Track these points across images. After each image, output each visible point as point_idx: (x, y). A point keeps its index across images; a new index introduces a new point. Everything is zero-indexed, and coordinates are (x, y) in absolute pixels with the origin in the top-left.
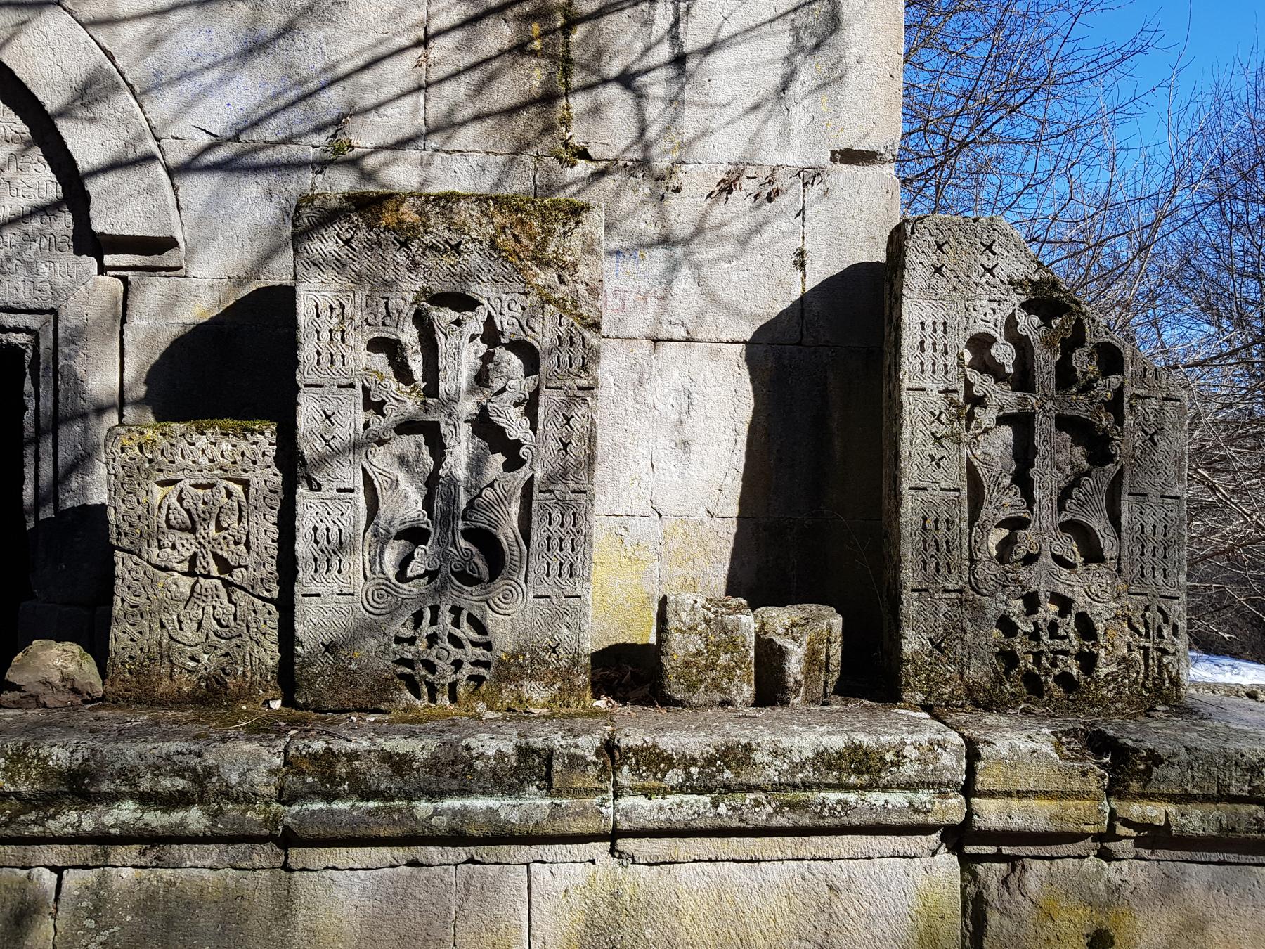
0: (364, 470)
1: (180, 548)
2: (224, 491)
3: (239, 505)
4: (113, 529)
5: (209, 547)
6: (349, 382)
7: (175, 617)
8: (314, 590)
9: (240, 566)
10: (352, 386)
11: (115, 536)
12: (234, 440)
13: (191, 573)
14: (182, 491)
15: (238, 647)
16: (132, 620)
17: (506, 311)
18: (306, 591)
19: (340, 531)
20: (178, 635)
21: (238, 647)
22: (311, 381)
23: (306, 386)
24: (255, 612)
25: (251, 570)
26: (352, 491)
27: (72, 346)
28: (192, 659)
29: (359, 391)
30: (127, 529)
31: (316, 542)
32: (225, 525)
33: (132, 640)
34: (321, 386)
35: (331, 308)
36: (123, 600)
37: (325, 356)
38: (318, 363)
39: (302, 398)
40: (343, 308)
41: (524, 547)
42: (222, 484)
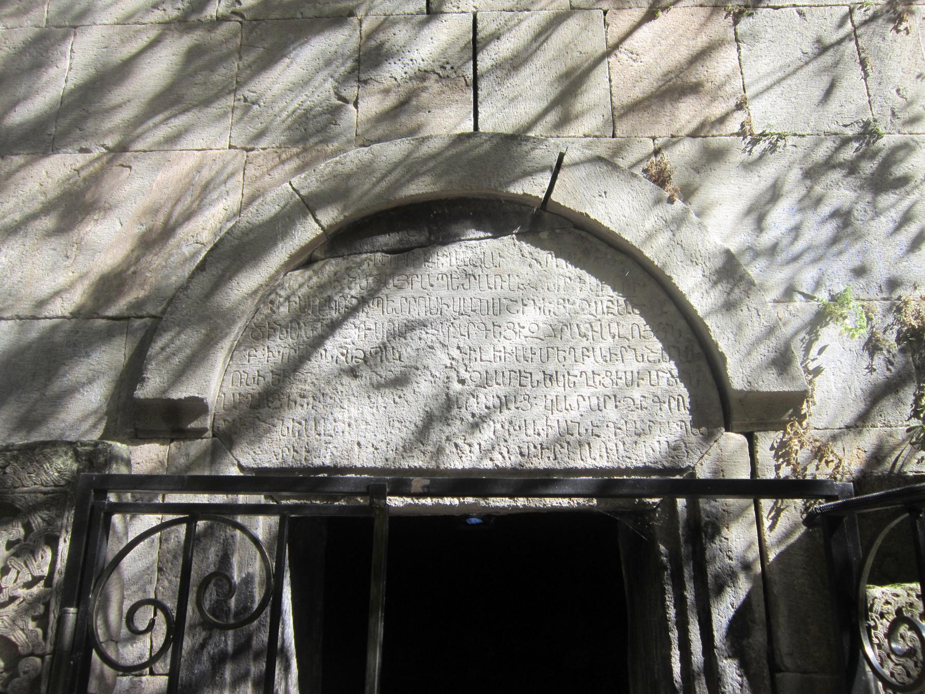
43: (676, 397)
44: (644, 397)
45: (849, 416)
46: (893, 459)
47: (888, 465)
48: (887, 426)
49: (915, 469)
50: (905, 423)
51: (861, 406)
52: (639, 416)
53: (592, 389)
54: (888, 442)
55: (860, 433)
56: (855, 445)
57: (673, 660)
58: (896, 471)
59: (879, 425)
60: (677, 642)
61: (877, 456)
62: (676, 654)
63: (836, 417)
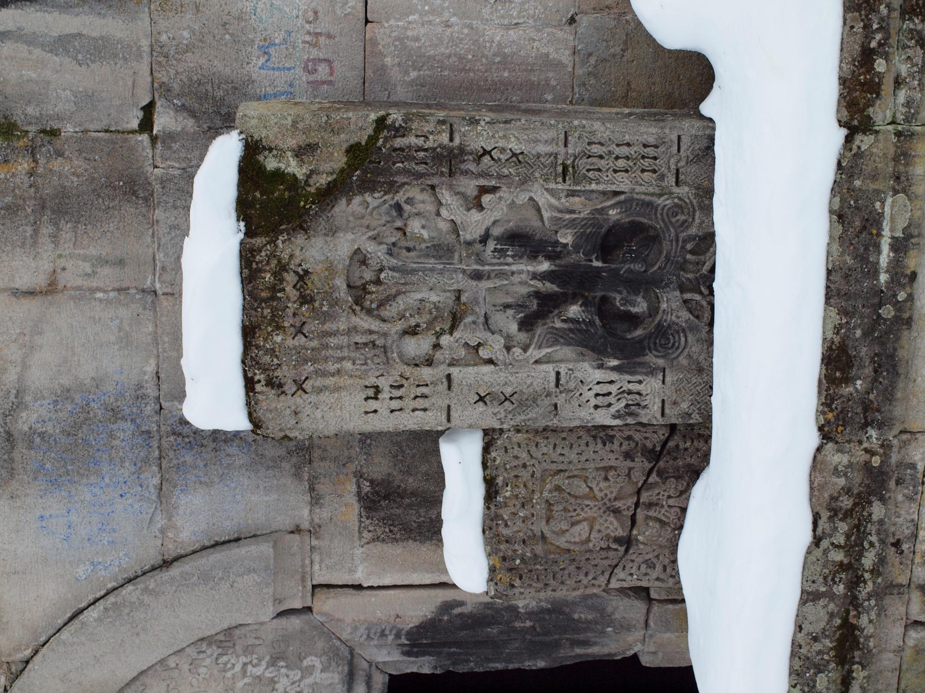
0: (536, 362)
2: (556, 494)
3: (569, 477)
8: (657, 407)
10: (449, 377)
14: (553, 532)
17: (365, 222)
18: (659, 416)
19: (598, 383)
22: (444, 416)
23: (449, 420)
26: (558, 373)
27: (387, 632)
29: (454, 371)
31: (610, 405)
34: (449, 406)
35: (367, 399)
38: (425, 410)
40: (366, 387)
41: (622, 197)
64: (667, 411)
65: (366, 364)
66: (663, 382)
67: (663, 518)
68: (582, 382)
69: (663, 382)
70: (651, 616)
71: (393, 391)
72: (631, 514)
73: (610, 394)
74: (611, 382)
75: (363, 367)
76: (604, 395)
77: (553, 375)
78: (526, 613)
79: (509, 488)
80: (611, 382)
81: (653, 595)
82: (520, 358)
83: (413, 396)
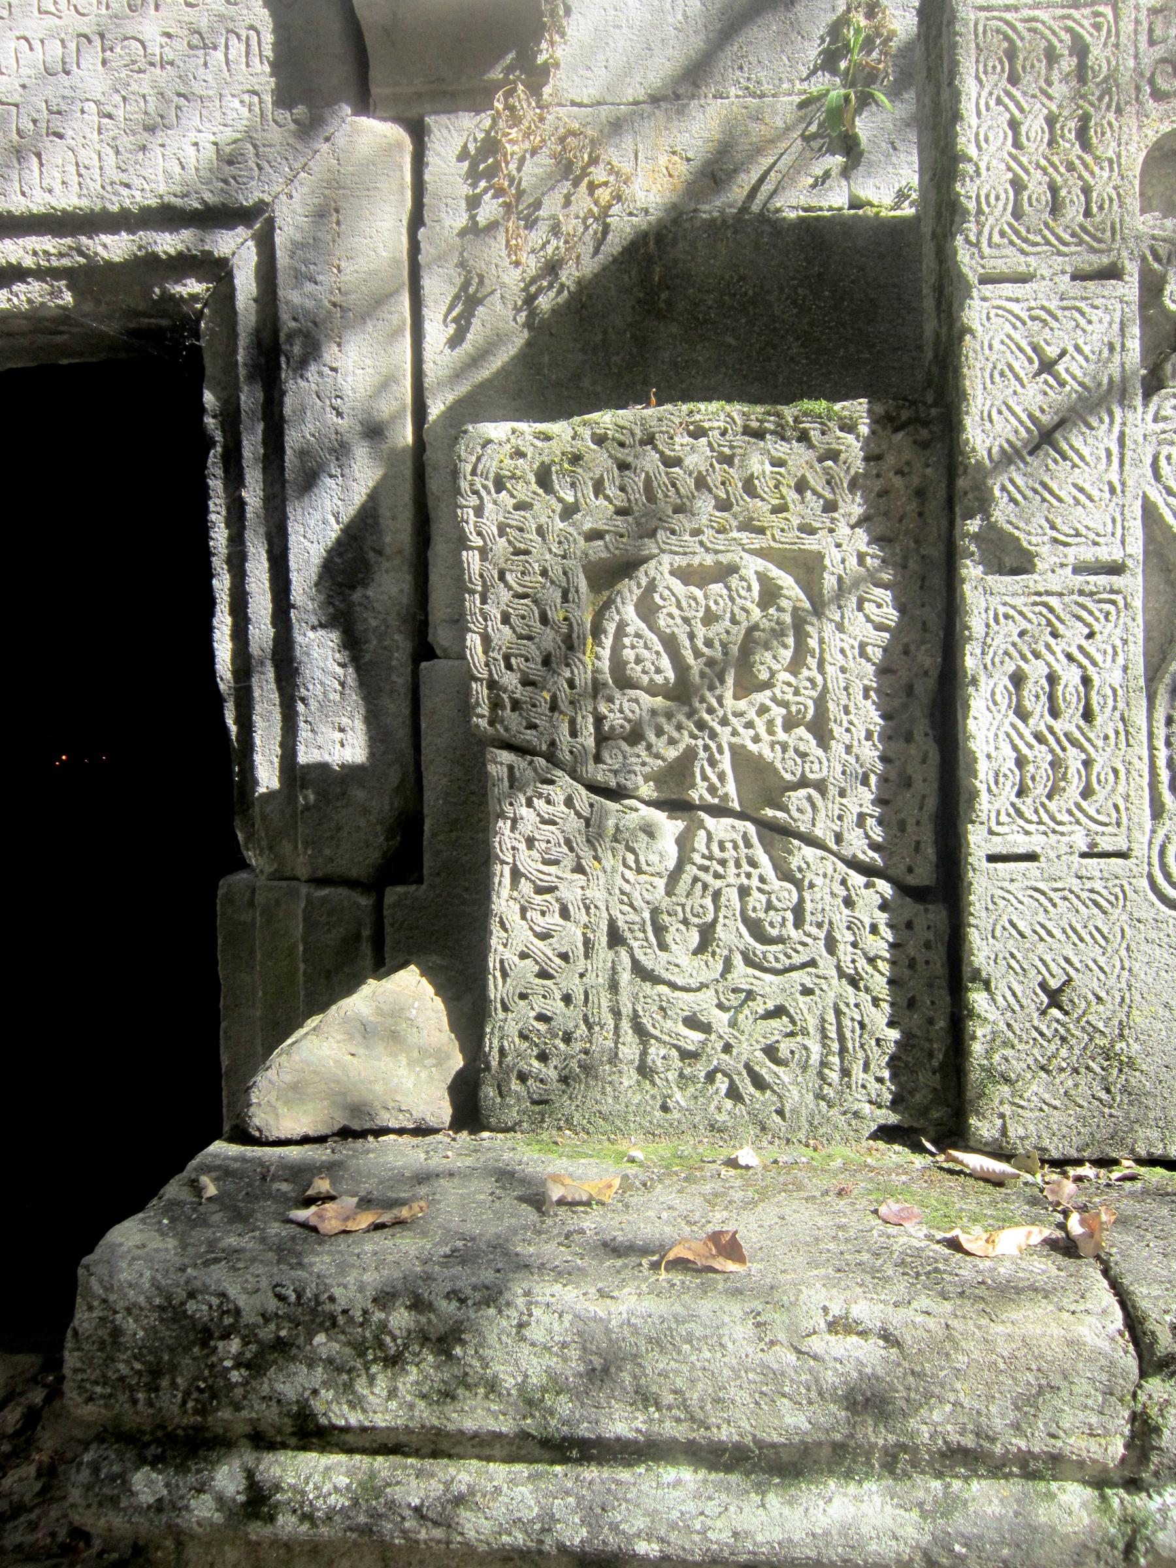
1: (651, 736)
4: (480, 691)
5: (724, 733)
6: (1105, 260)
7: (647, 915)
9: (803, 783)
10: (1112, 273)
11: (484, 710)
12: (780, 449)
13: (677, 806)
14: (651, 587)
15: (807, 992)
16: (542, 923)
19: (1086, 681)
20: (652, 960)
21: (807, 992)
24: (849, 903)
25: (833, 791)
26: (1115, 569)
28: (692, 1022)
29: (1129, 289)
30: (520, 693)
31: (1022, 714)
32: (764, 676)
33: (544, 974)
36: (516, 874)
37: (1036, 185)
38: (1017, 214)
39: (974, 313)
42: (752, 566)
43: (244, 33)
44: (168, 35)
45: (660, 68)
46: (755, 176)
47: (737, 192)
48: (754, 95)
49: (803, 201)
50: (798, 86)
51: (697, 43)
52: (154, 84)
53: (50, 21)
54: (747, 134)
55: (681, 112)
56: (665, 142)
57: (217, 635)
58: (756, 207)
59: (733, 91)
60: (227, 598)
61: (715, 172)
62: (223, 623)
63: (627, 72)
64: (999, 865)
65: (1152, 43)
66: (1084, 855)
67: (686, 878)
68: (1091, 635)
69: (1084, 855)
70: (343, 891)
71: (1072, 124)
72: (694, 795)
73: (1054, 713)
74: (1088, 715)
75: (1143, 39)
76: (1051, 697)
77: (1117, 555)
78: (351, 605)
79: (768, 468)
80: (1088, 715)
81: (393, 894)
82: (1163, 462)
83: (1058, 179)
